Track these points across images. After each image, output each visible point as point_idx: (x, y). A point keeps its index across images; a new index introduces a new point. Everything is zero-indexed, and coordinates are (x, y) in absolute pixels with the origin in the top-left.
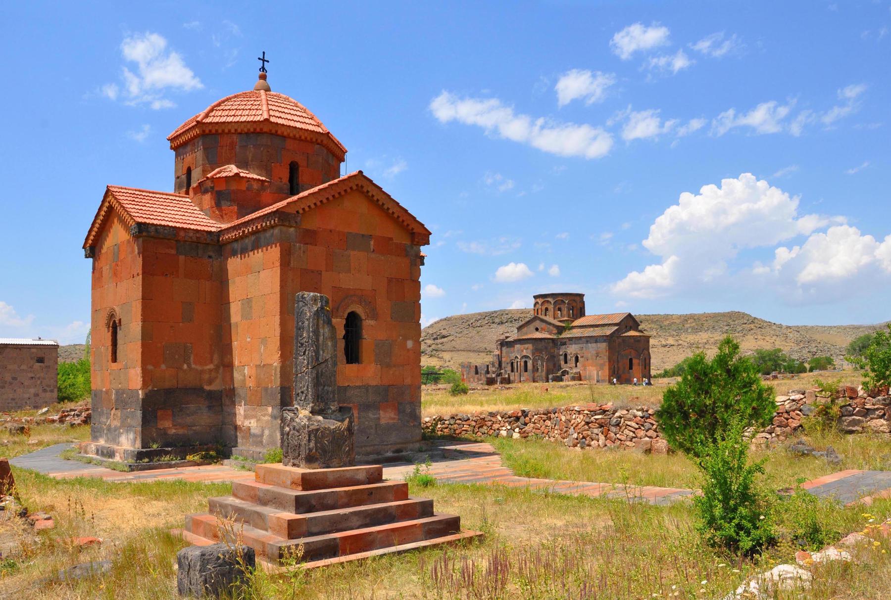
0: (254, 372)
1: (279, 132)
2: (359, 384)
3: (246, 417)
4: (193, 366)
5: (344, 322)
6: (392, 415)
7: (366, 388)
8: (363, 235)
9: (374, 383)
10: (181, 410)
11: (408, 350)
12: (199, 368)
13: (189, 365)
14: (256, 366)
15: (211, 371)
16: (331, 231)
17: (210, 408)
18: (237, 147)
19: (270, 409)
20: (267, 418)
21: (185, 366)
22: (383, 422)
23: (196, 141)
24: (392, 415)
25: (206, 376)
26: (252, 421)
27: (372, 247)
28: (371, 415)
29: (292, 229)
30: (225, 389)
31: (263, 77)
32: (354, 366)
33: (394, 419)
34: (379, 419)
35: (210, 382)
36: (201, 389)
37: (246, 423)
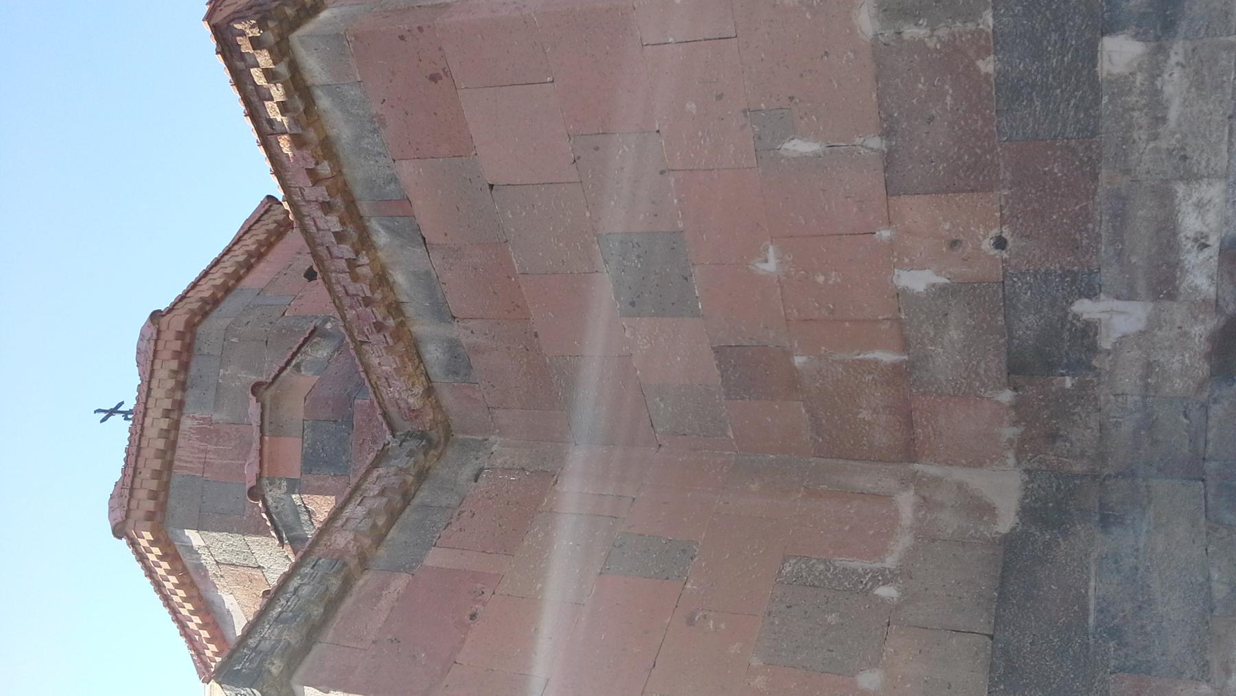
0: (916, 210)
3: (1164, 284)
4: (890, 562)
10: (1115, 633)
12: (903, 542)
13: (884, 577)
14: (891, 189)
15: (925, 503)
17: (1107, 520)
18: (216, 417)
19: (1120, 52)
20: (1174, 84)
21: (887, 592)
23: (188, 560)
25: (949, 521)
26: (1190, 223)
30: (1020, 455)
35: (981, 509)
36: (1011, 545)
37: (1200, 274)
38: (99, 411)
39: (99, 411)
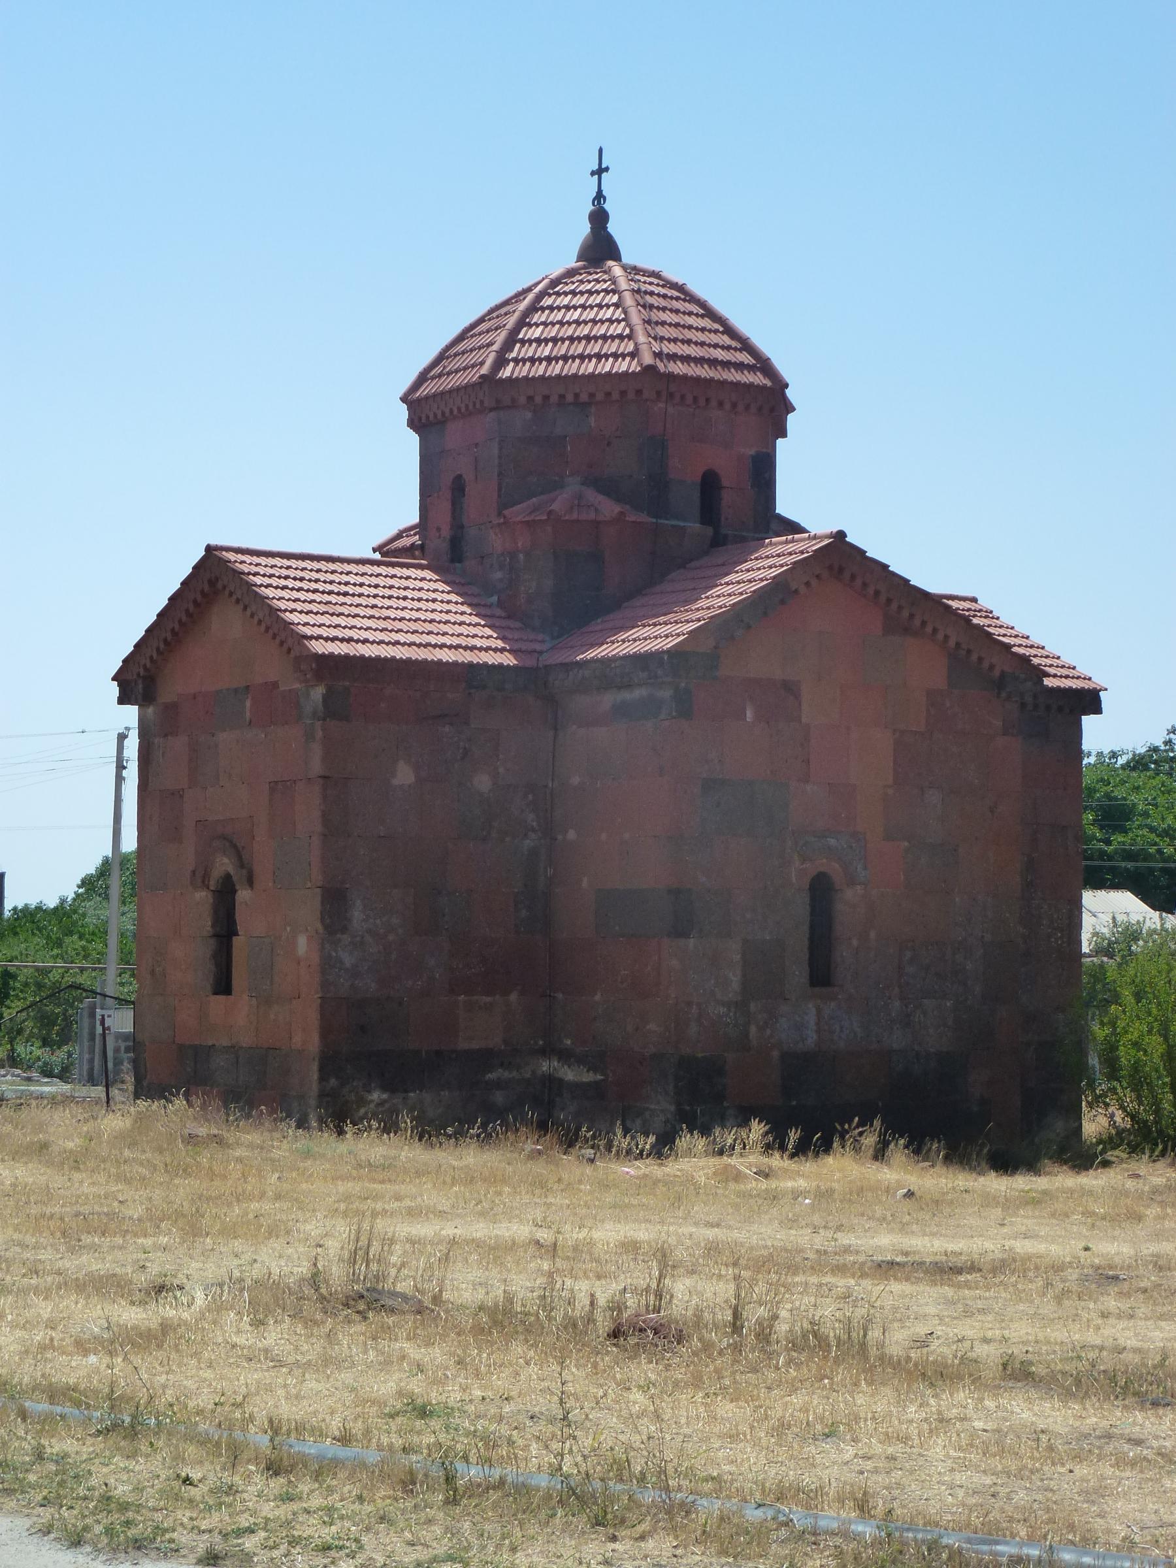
8: (236, 691)
9: (246, 1040)
31: (599, 218)
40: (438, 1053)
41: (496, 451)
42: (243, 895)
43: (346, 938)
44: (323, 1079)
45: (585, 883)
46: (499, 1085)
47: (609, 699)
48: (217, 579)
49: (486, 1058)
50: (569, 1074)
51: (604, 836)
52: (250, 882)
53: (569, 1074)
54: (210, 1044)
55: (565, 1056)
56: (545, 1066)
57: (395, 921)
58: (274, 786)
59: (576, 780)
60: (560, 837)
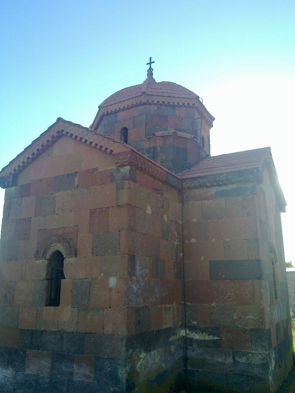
1: (109, 111)
2: (54, 329)
5: (46, 262)
6: (88, 372)
7: (61, 334)
8: (68, 175)
9: (70, 329)
11: (110, 289)
16: (41, 180)
22: (76, 378)
24: (88, 372)
27: (76, 184)
28: (64, 368)
29: (13, 188)
32: (52, 308)
33: (89, 377)
34: (72, 374)
38: (151, 58)
39: (151, 58)
40: (158, 331)
41: (145, 118)
42: (68, 261)
43: (135, 278)
44: (127, 350)
45: (202, 258)
46: (172, 343)
47: (213, 191)
48: (63, 131)
49: (170, 331)
50: (197, 336)
51: (214, 240)
52: (76, 254)
53: (197, 336)
54: (42, 329)
55: (193, 328)
56: (183, 333)
57: (148, 271)
58: (93, 212)
59: (195, 220)
60: (187, 241)
